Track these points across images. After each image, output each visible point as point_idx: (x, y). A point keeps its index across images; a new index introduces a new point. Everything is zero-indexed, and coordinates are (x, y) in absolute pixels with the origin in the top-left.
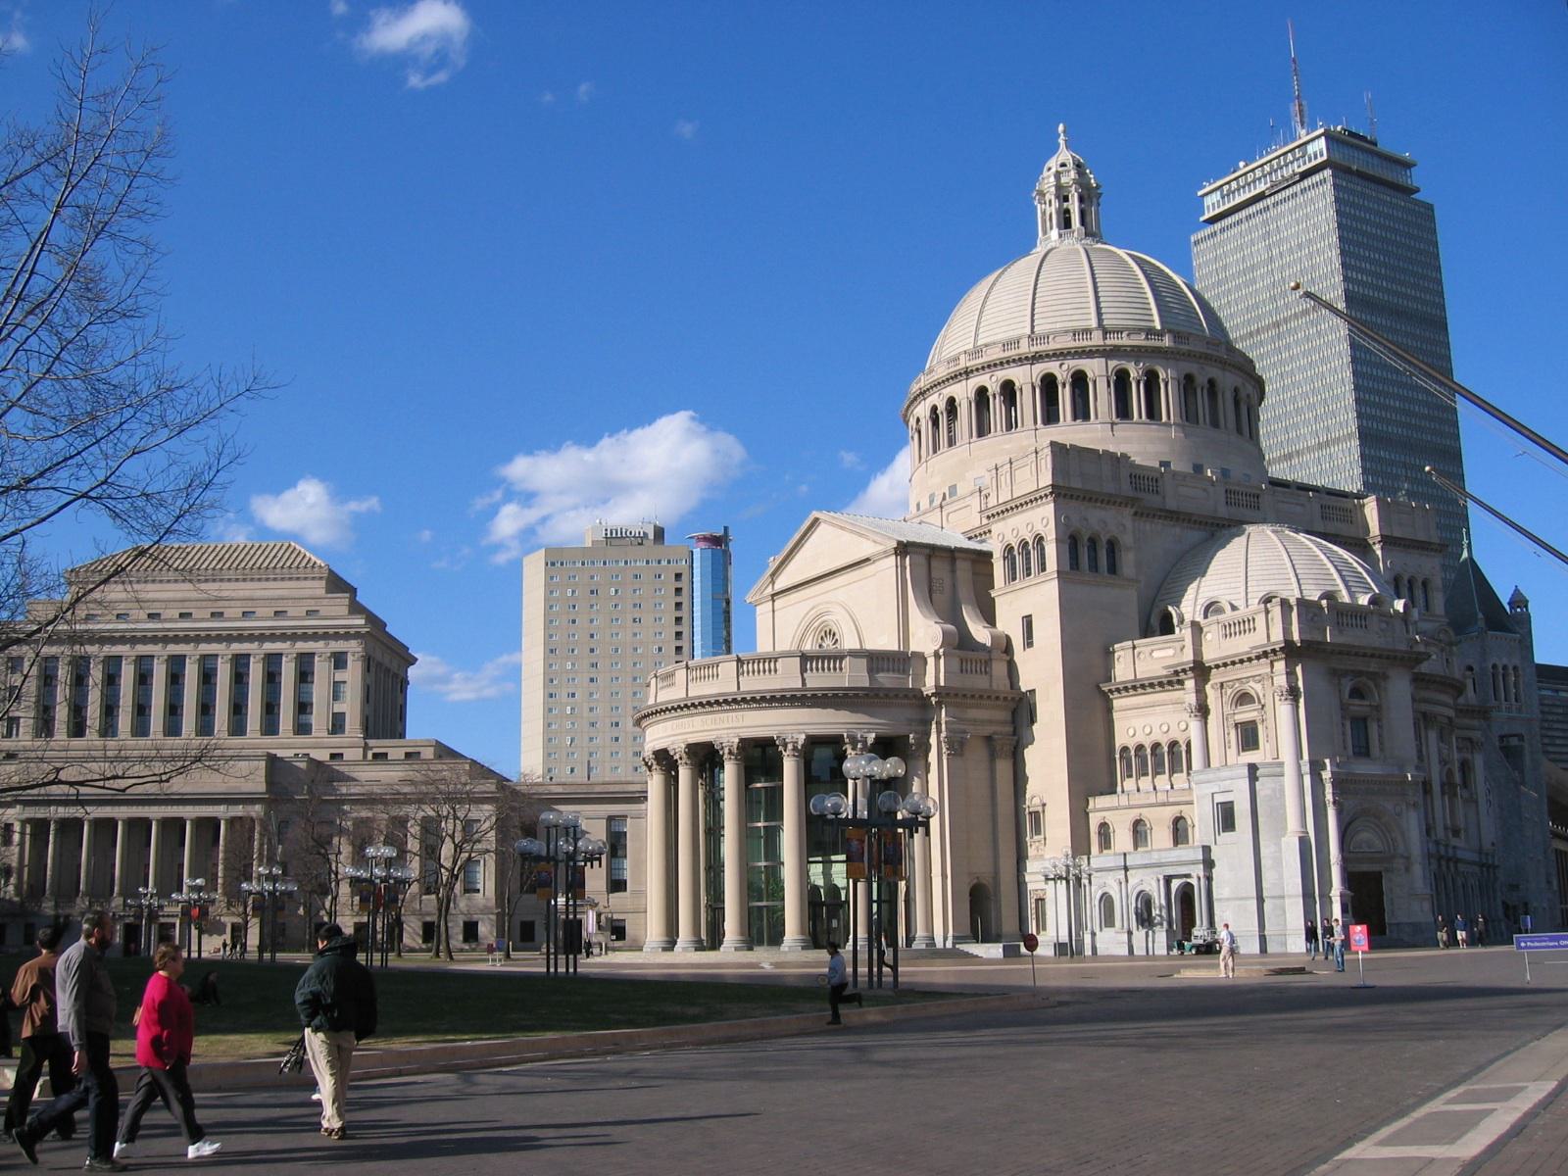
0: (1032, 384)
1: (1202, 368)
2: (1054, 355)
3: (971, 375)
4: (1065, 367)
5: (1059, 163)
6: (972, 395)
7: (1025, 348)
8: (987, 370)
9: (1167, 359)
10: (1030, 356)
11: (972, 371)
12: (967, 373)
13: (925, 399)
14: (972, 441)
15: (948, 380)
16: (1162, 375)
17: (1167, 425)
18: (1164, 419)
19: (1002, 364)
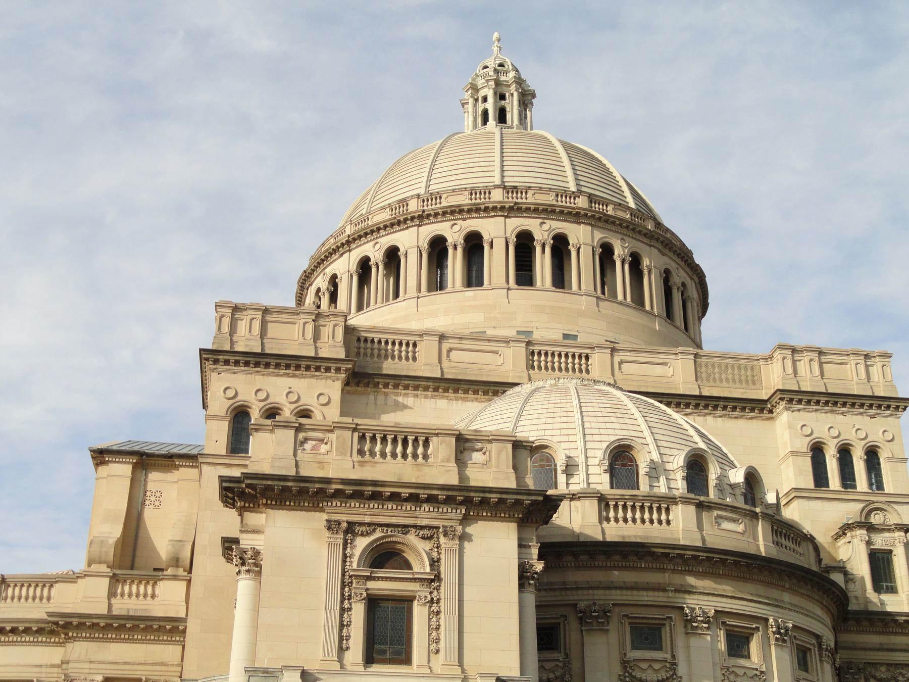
0: (506, 239)
1: (677, 268)
2: (536, 210)
3: (425, 221)
4: (546, 227)
5: (498, 62)
6: (425, 245)
7: (497, 196)
8: (449, 217)
9: (650, 246)
10: (507, 206)
11: (429, 216)
12: (422, 218)
13: (350, 251)
14: (420, 295)
15: (392, 225)
16: (646, 262)
17: (651, 314)
18: (648, 307)
19: (469, 211)
